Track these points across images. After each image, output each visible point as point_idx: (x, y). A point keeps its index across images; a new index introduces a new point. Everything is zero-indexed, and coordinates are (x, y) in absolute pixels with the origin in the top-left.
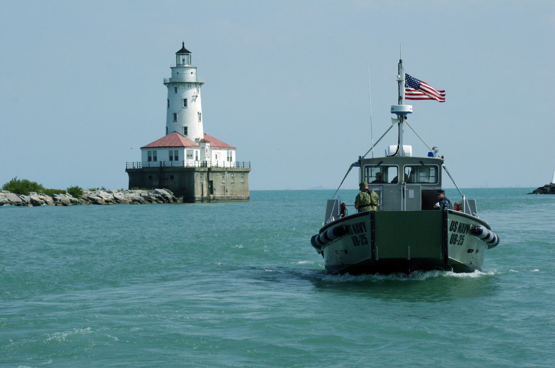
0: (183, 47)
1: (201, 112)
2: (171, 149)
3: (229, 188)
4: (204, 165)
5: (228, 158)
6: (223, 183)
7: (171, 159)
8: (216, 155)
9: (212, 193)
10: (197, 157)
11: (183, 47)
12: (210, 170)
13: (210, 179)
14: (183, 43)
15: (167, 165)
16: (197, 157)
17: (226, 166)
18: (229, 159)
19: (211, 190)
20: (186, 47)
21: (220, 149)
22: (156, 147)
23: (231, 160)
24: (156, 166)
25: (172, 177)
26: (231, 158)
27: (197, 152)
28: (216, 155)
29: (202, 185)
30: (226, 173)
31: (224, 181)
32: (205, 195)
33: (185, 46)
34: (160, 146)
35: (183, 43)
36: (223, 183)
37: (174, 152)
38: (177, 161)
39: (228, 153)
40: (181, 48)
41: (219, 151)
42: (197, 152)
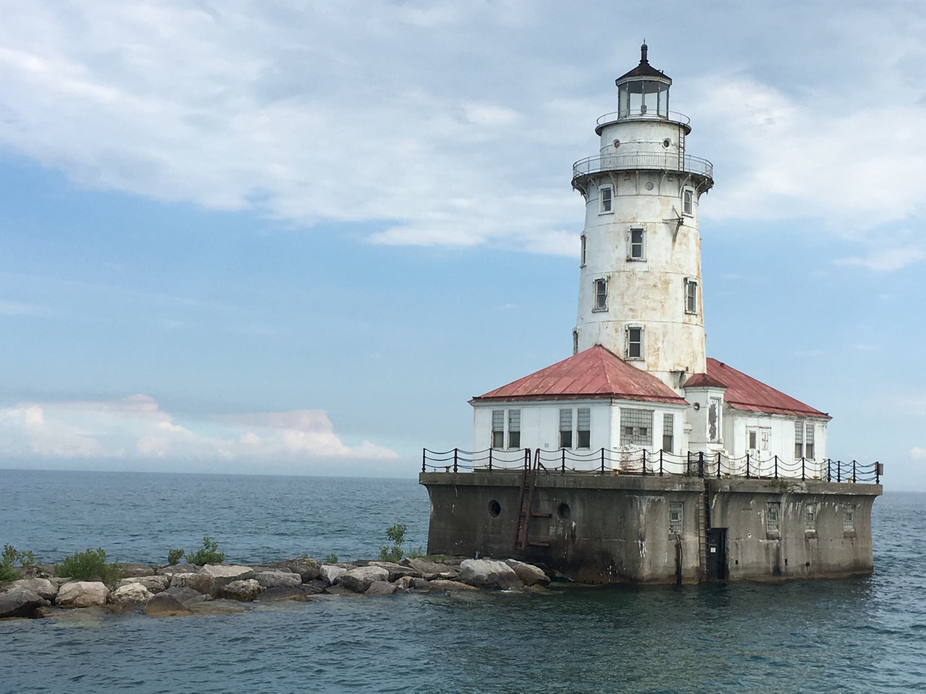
0: (644, 61)
1: (693, 275)
2: (566, 405)
4: (696, 466)
5: (799, 446)
6: (769, 537)
7: (566, 441)
8: (753, 436)
10: (668, 439)
11: (644, 61)
12: (711, 488)
13: (716, 524)
14: (644, 49)
15: (549, 466)
16: (668, 439)
17: (782, 473)
20: (653, 63)
21: (769, 415)
22: (518, 398)
23: (811, 455)
24: (510, 466)
25: (563, 509)
26: (810, 447)
27: (669, 419)
28: (753, 436)
29: (678, 547)
30: (783, 500)
34: (535, 392)
35: (644, 49)
37: (575, 415)
38: (584, 451)
39: (799, 433)
40: (636, 63)
41: (765, 421)
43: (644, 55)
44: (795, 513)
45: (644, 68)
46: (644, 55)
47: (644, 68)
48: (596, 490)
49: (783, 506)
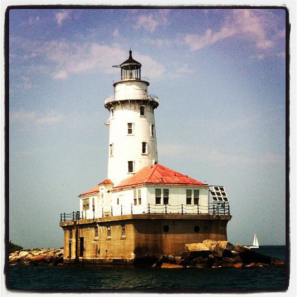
0: (131, 57)
3: (103, 247)
9: (82, 255)
11: (131, 57)
13: (81, 237)
14: (131, 52)
18: (137, 201)
19: (81, 250)
26: (140, 199)
27: (93, 199)
31: (97, 238)
32: (74, 257)
33: (132, 56)
35: (131, 52)
36: (95, 240)
41: (122, 193)
42: (93, 199)
43: (131, 55)
44: (103, 231)
45: (131, 60)
46: (131, 55)
47: (131, 60)
48: (197, 220)
49: (99, 227)
